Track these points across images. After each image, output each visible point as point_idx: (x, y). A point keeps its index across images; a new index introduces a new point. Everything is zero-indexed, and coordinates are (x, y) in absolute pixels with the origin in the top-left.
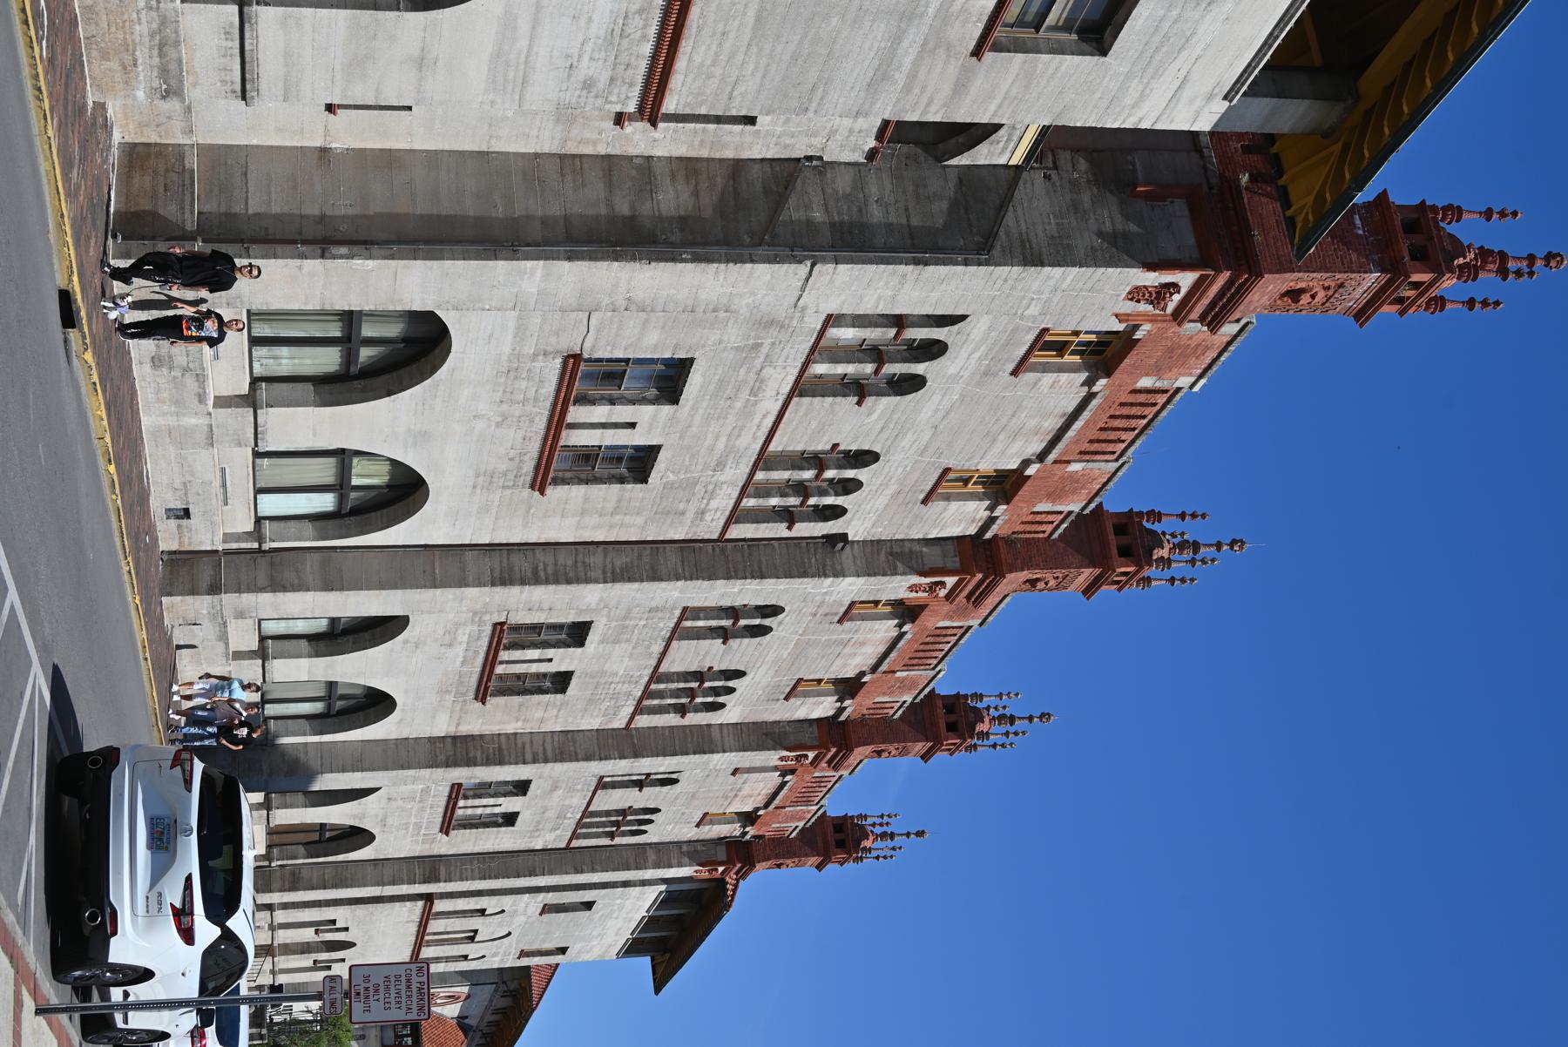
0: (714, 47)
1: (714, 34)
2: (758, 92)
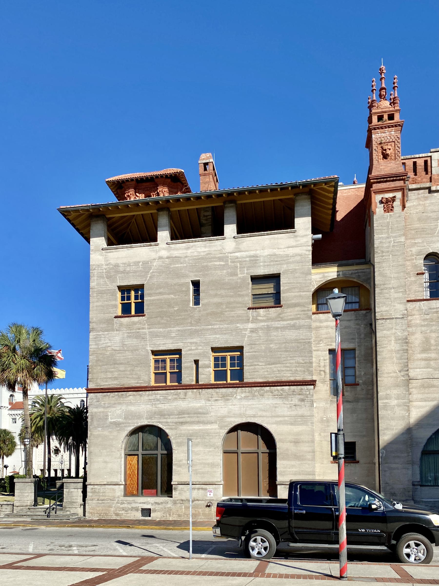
0: (284, 372)
1: (279, 373)
2: (302, 357)
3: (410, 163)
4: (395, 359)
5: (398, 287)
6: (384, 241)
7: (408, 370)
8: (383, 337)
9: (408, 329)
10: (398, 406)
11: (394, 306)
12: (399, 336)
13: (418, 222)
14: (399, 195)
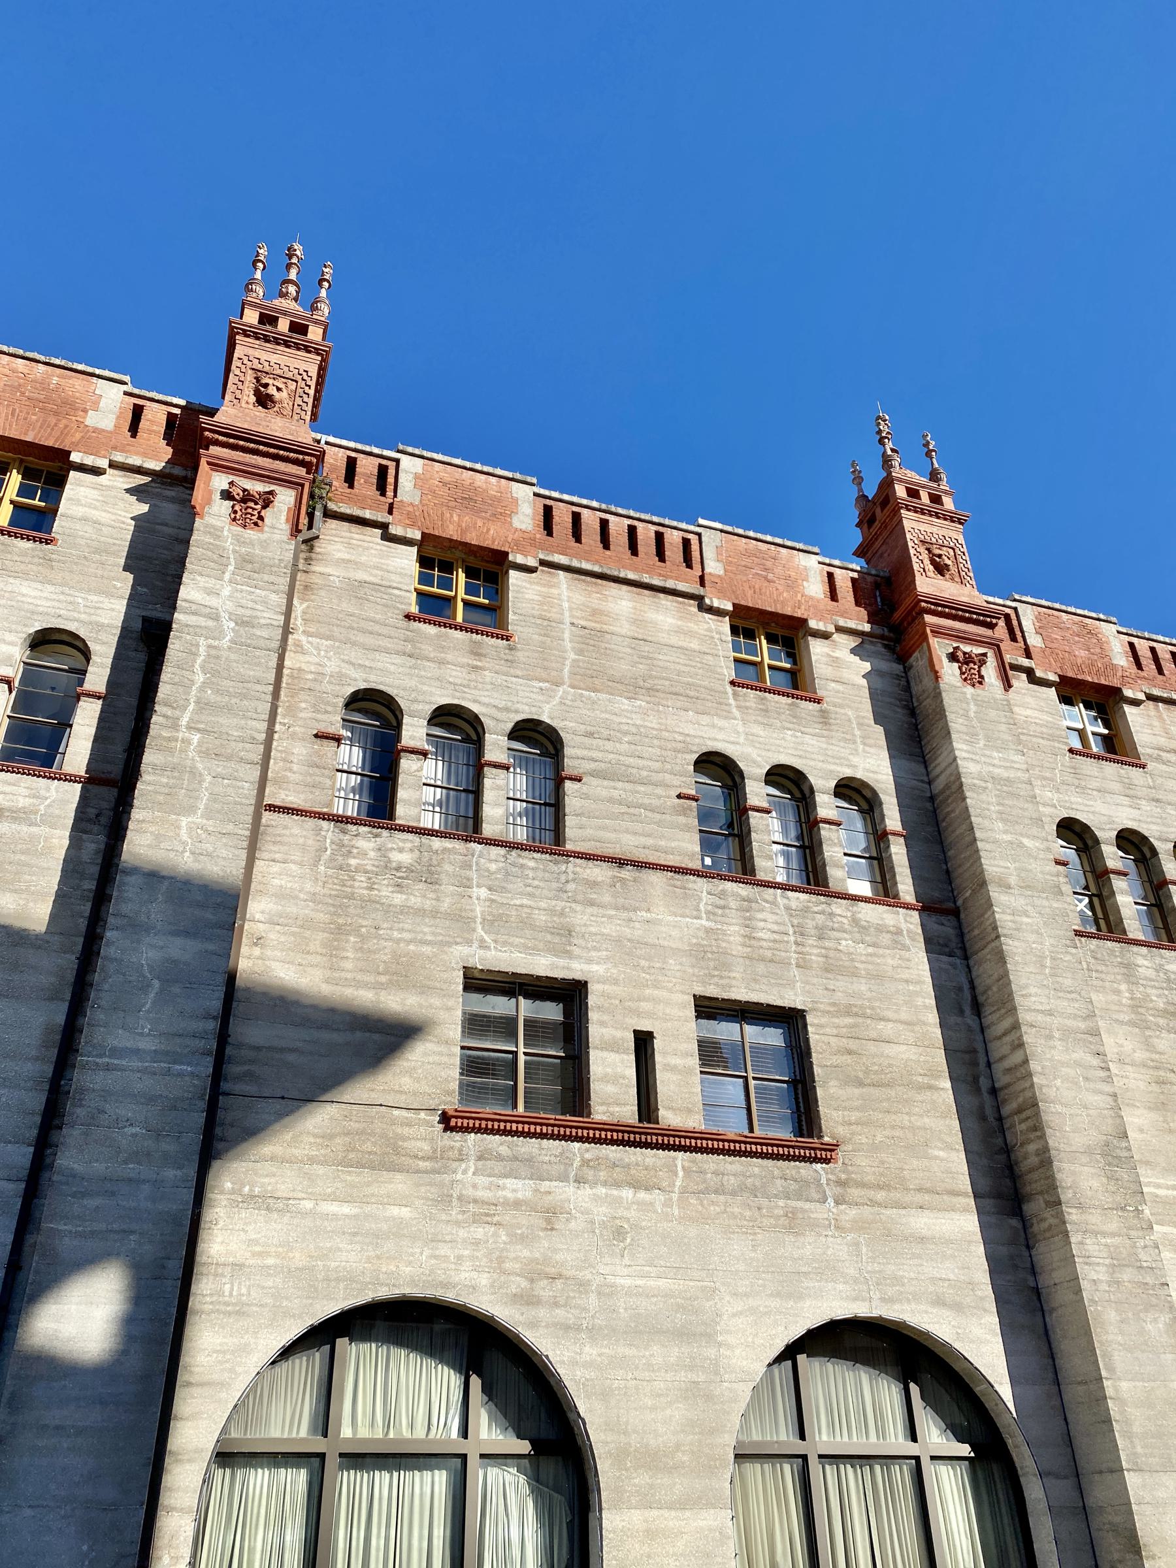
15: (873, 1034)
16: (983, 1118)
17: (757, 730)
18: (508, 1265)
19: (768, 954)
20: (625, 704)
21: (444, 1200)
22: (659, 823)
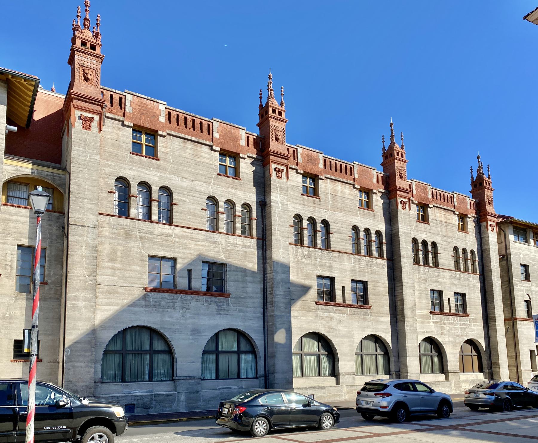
3: (107, 94)
4: (85, 264)
5: (91, 199)
6: (81, 154)
7: (96, 276)
8: (75, 242)
9: (98, 239)
10: (86, 307)
11: (87, 215)
12: (90, 243)
13: (112, 147)
14: (96, 118)
15: (377, 286)
16: (392, 301)
17: (363, 219)
18: (326, 327)
19: (362, 270)
20: (340, 214)
21: (317, 316)
22: (346, 243)
